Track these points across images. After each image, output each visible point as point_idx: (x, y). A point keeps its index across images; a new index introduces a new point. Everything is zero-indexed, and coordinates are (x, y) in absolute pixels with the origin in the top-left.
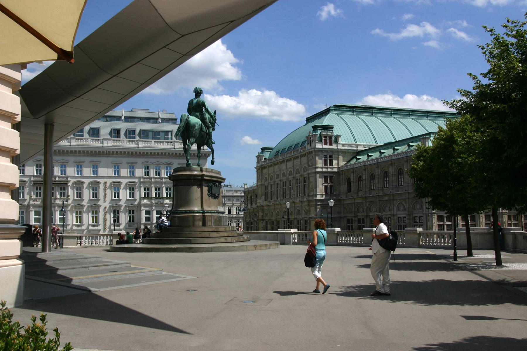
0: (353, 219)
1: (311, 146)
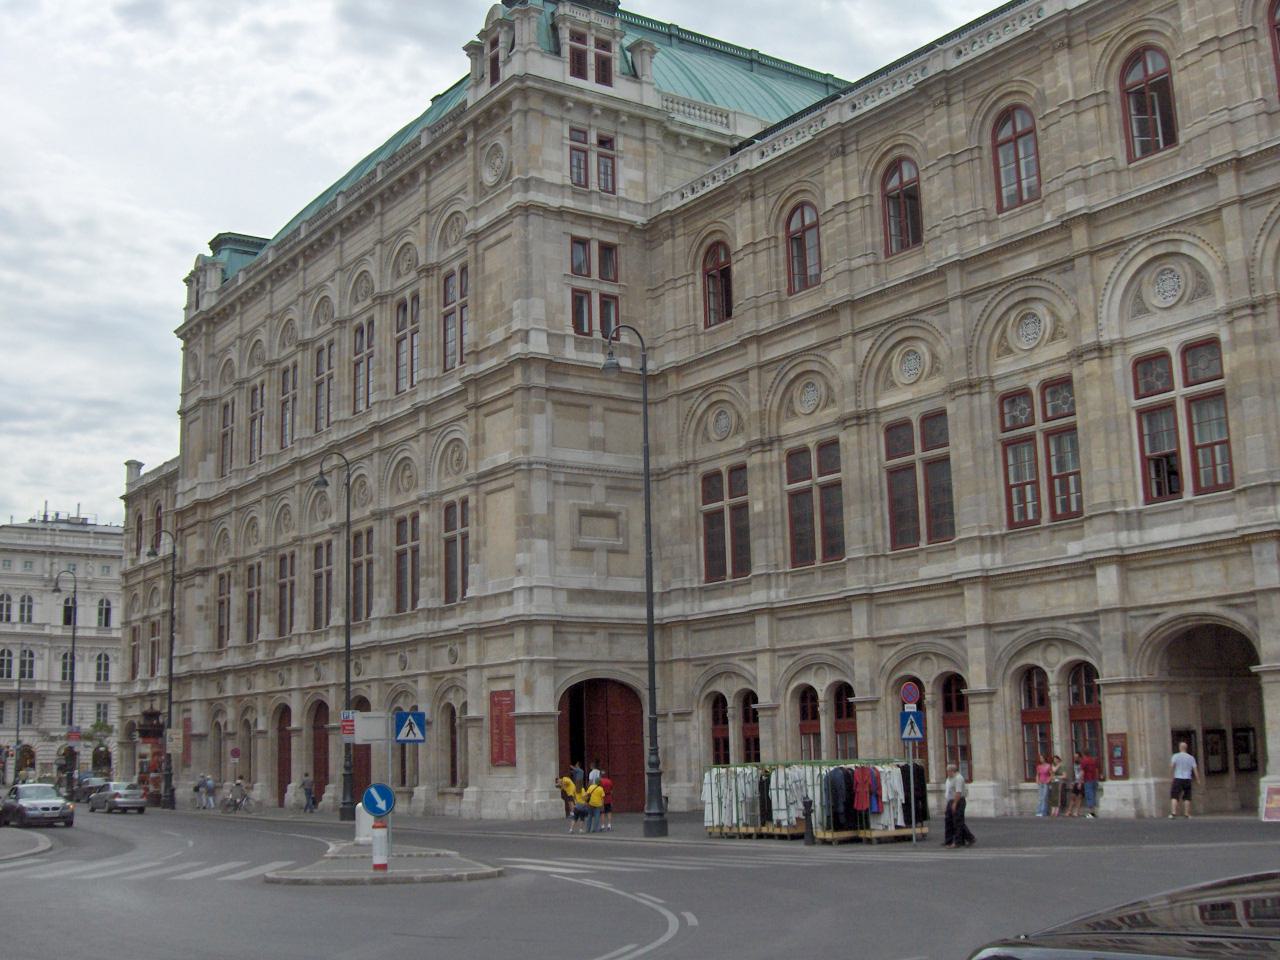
0: (754, 460)
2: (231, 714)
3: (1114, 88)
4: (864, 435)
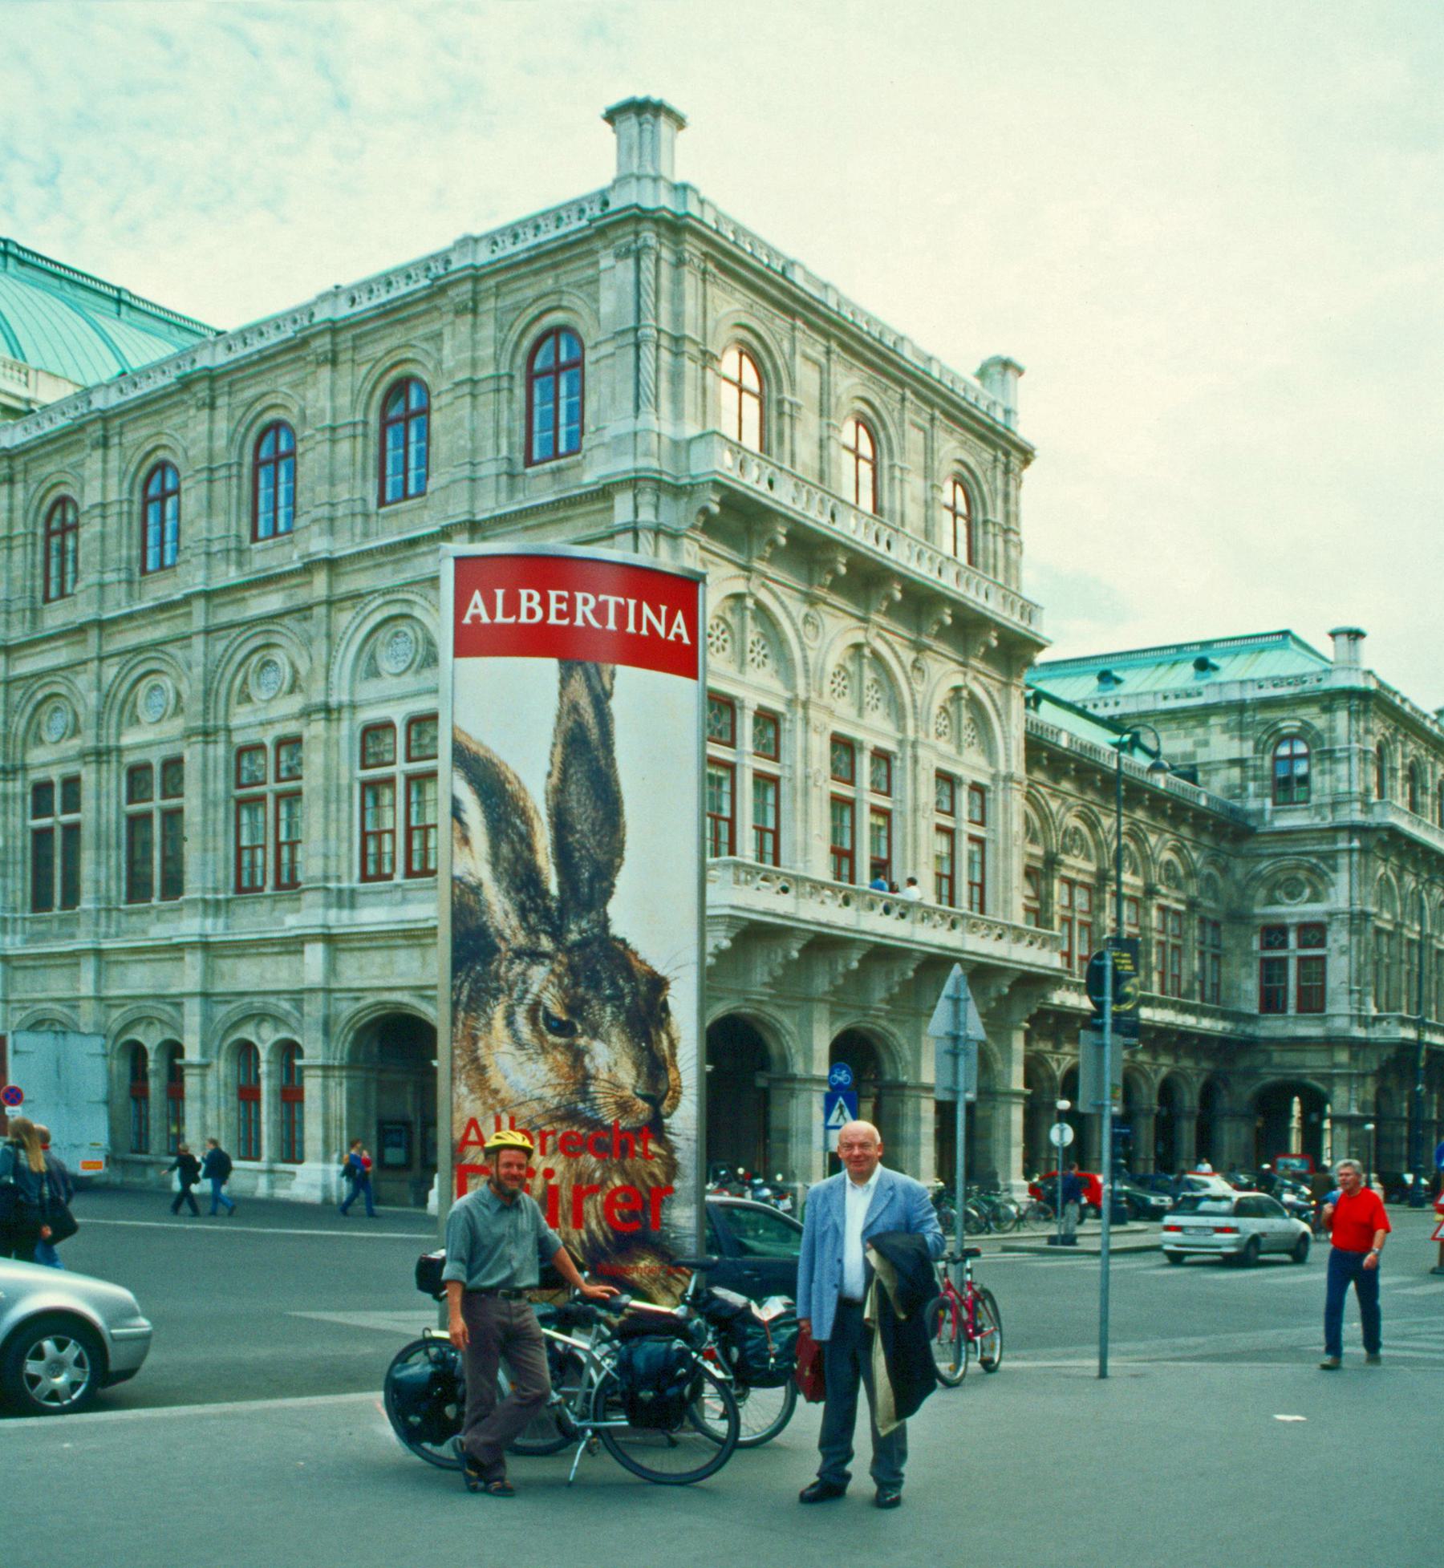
3: (374, 418)
4: (104, 774)
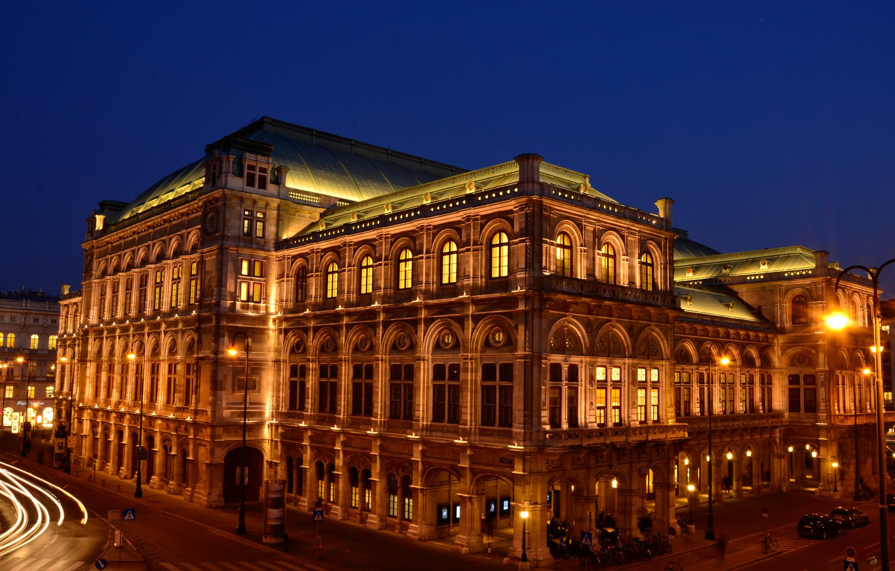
1: (214, 184)
2: (100, 429)
